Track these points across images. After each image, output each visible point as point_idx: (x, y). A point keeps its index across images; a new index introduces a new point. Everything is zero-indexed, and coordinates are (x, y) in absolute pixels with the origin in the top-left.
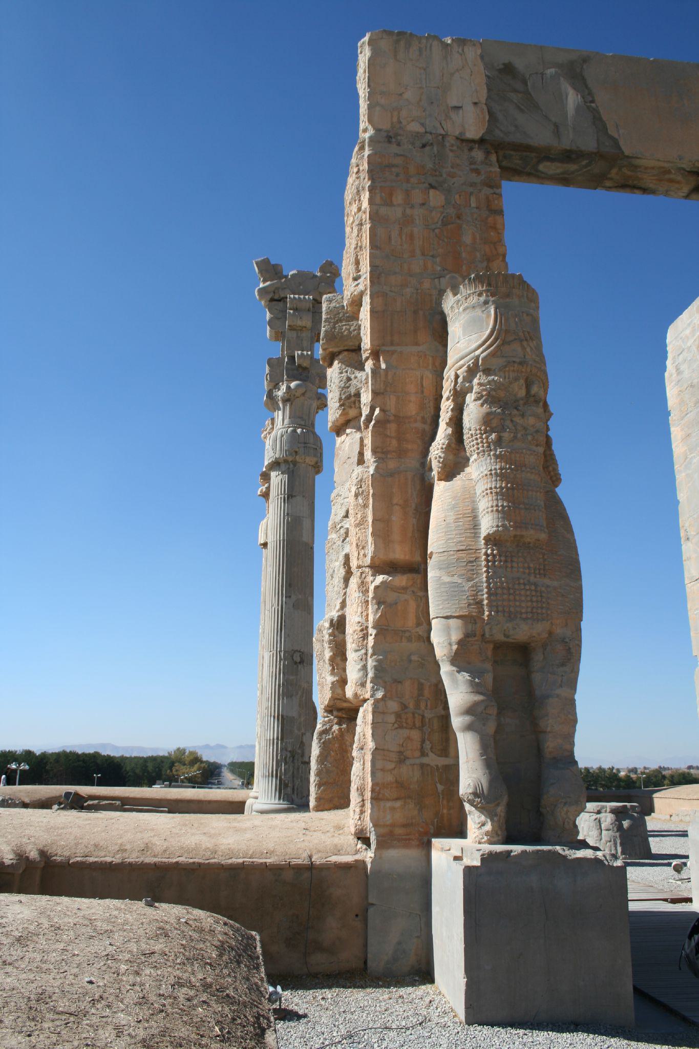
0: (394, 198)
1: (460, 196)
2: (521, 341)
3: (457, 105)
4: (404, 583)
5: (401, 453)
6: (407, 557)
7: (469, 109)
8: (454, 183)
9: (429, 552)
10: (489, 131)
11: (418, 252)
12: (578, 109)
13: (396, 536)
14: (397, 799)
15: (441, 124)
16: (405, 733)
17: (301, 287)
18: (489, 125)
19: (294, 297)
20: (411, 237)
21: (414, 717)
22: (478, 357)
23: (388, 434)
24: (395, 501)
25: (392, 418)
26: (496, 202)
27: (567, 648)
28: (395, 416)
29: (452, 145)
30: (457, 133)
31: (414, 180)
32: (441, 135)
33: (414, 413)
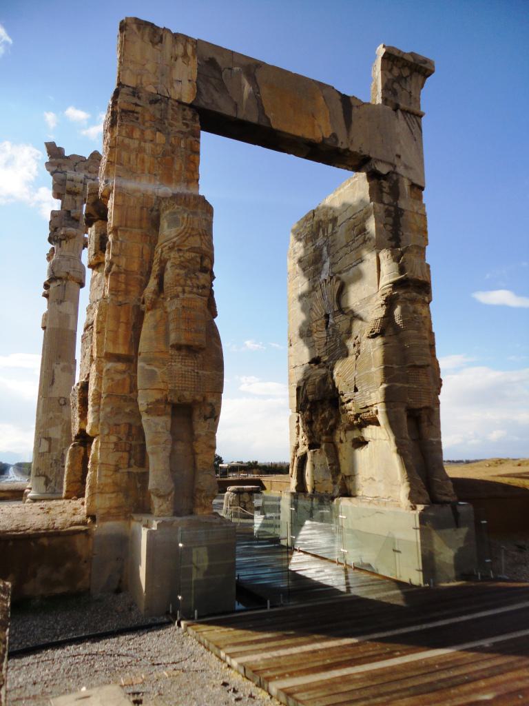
0: (134, 135)
2: (200, 235)
4: (124, 368)
5: (127, 292)
6: (126, 353)
7: (186, 82)
9: (139, 351)
10: (196, 100)
12: (250, 95)
13: (121, 340)
14: (113, 493)
16: (120, 454)
18: (197, 96)
20: (143, 161)
21: (125, 445)
22: (174, 243)
24: (121, 320)
25: (123, 271)
28: (125, 270)
29: (173, 106)
30: (177, 98)
31: (147, 124)
33: (136, 269)
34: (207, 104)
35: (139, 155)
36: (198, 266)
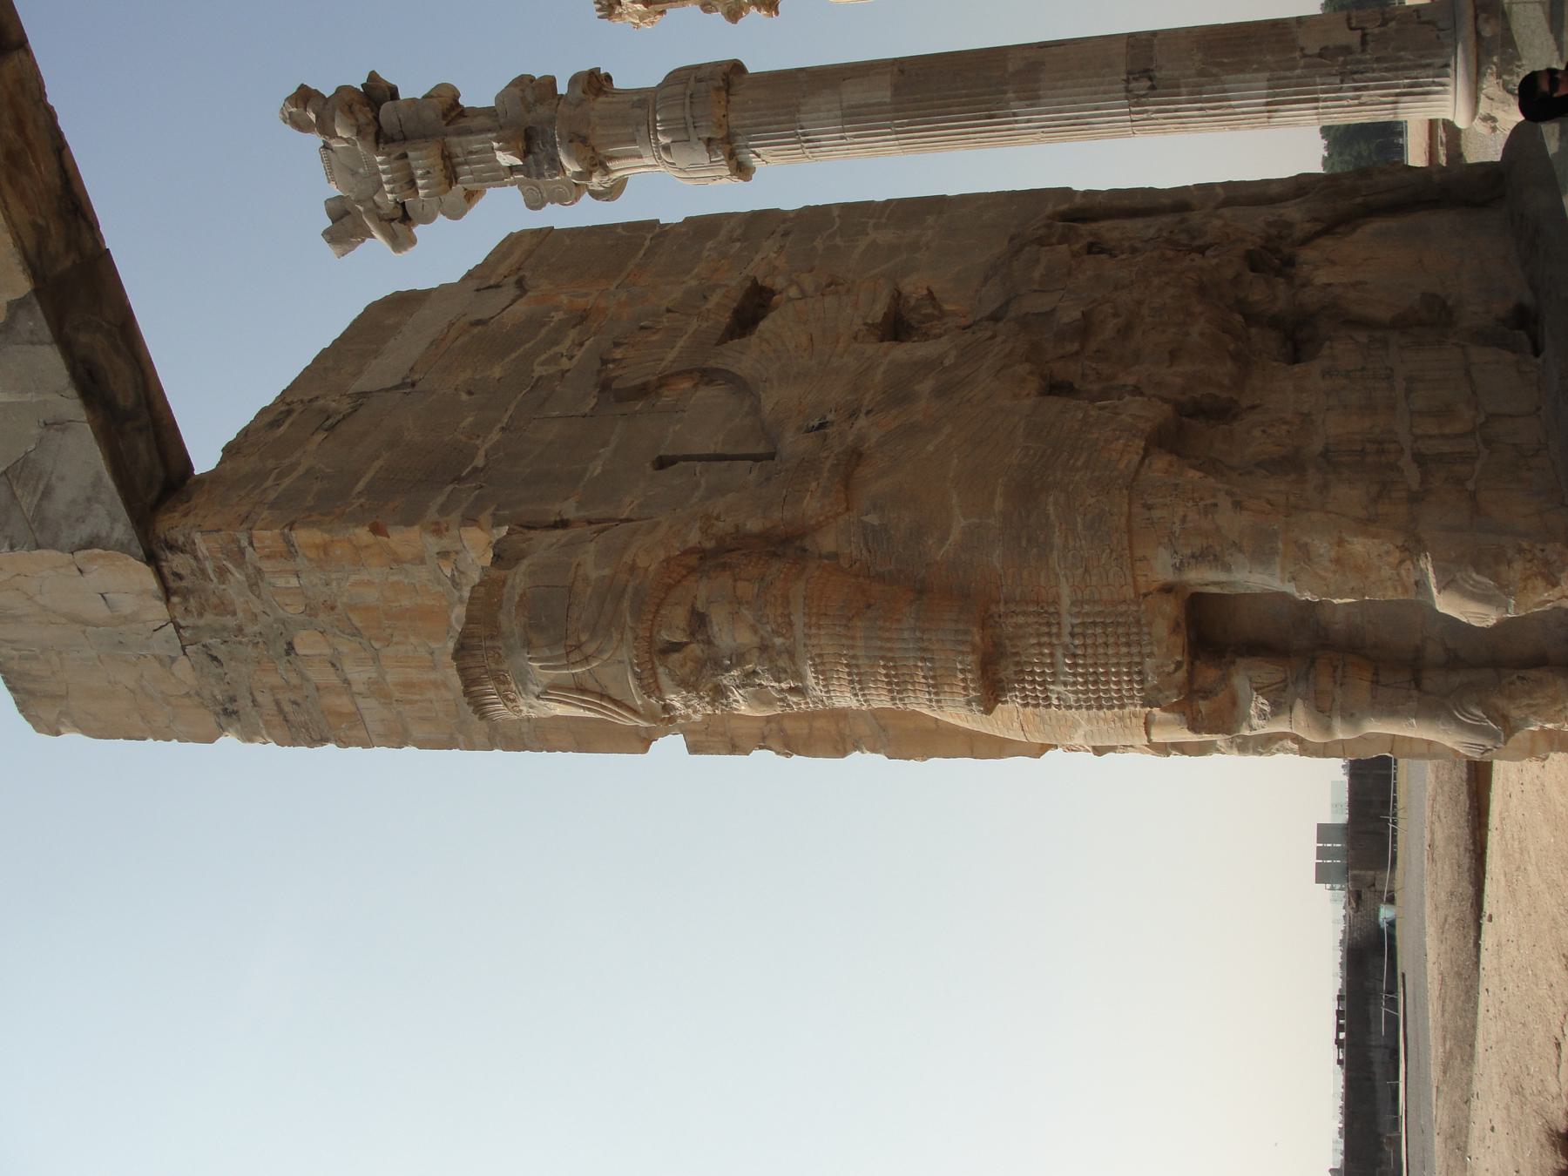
1: (287, 605)
3: (103, 602)
8: (264, 612)
10: (123, 548)
11: (433, 676)
15: (155, 630)
17: (361, 170)
19: (391, 192)
20: (408, 685)
23: (806, 731)
26: (268, 542)
27: (1193, 561)
30: (161, 605)
32: (178, 632)
34: (114, 520)
35: (397, 695)
36: (696, 649)
